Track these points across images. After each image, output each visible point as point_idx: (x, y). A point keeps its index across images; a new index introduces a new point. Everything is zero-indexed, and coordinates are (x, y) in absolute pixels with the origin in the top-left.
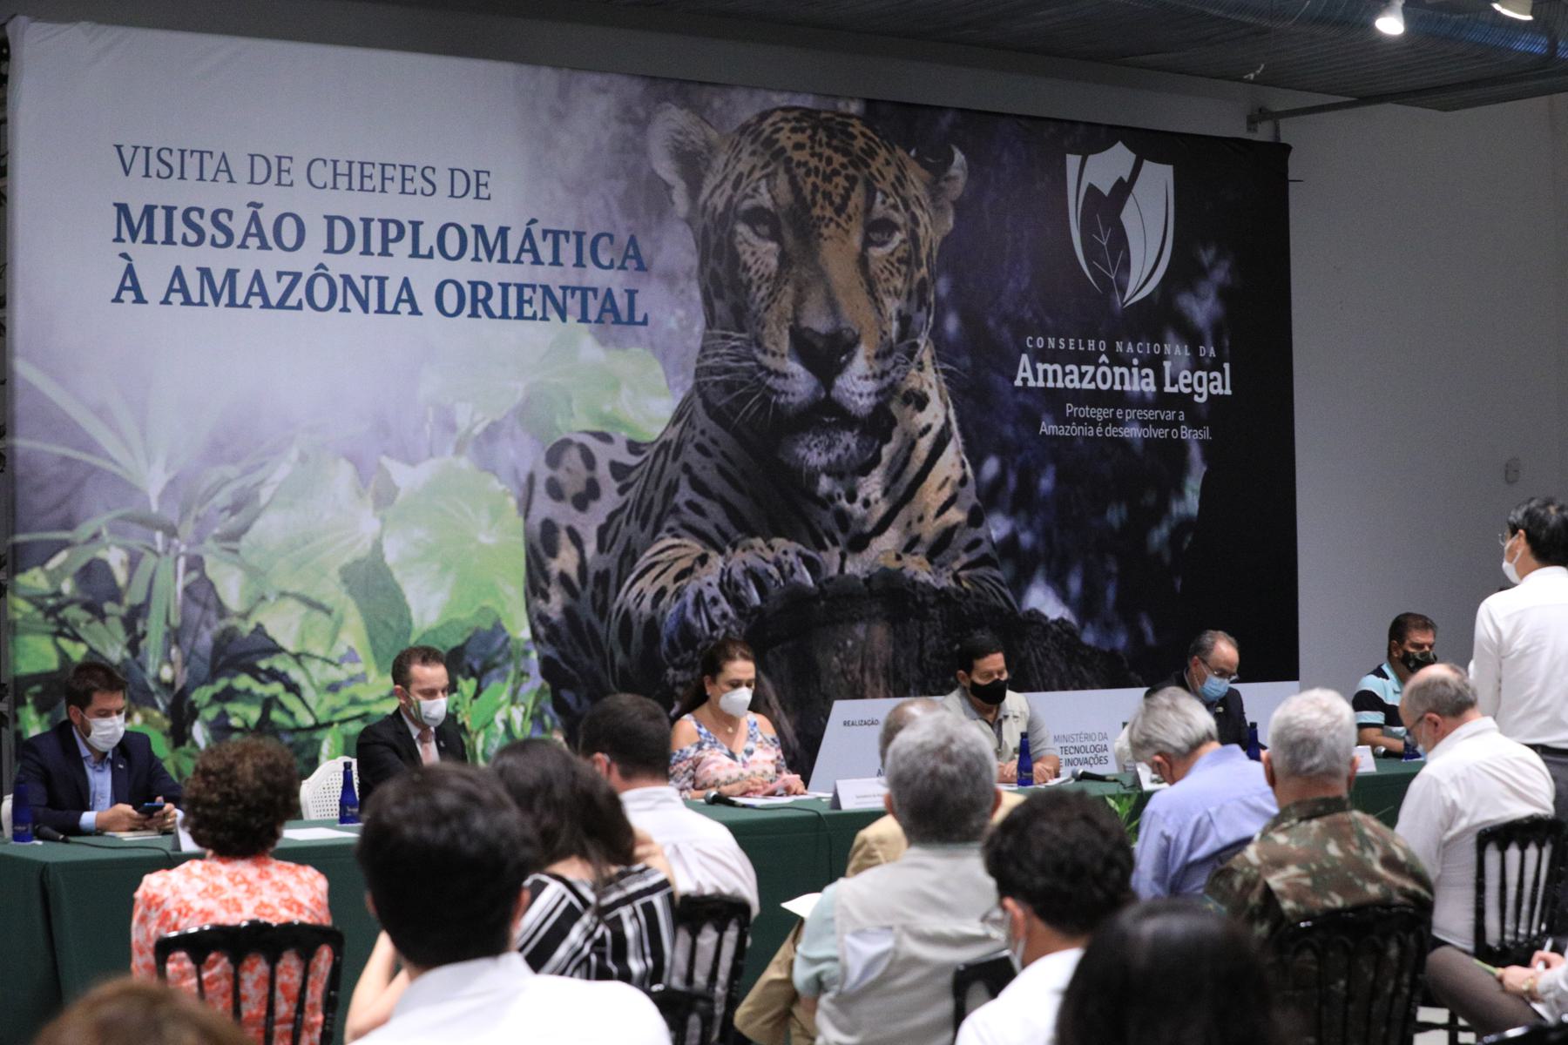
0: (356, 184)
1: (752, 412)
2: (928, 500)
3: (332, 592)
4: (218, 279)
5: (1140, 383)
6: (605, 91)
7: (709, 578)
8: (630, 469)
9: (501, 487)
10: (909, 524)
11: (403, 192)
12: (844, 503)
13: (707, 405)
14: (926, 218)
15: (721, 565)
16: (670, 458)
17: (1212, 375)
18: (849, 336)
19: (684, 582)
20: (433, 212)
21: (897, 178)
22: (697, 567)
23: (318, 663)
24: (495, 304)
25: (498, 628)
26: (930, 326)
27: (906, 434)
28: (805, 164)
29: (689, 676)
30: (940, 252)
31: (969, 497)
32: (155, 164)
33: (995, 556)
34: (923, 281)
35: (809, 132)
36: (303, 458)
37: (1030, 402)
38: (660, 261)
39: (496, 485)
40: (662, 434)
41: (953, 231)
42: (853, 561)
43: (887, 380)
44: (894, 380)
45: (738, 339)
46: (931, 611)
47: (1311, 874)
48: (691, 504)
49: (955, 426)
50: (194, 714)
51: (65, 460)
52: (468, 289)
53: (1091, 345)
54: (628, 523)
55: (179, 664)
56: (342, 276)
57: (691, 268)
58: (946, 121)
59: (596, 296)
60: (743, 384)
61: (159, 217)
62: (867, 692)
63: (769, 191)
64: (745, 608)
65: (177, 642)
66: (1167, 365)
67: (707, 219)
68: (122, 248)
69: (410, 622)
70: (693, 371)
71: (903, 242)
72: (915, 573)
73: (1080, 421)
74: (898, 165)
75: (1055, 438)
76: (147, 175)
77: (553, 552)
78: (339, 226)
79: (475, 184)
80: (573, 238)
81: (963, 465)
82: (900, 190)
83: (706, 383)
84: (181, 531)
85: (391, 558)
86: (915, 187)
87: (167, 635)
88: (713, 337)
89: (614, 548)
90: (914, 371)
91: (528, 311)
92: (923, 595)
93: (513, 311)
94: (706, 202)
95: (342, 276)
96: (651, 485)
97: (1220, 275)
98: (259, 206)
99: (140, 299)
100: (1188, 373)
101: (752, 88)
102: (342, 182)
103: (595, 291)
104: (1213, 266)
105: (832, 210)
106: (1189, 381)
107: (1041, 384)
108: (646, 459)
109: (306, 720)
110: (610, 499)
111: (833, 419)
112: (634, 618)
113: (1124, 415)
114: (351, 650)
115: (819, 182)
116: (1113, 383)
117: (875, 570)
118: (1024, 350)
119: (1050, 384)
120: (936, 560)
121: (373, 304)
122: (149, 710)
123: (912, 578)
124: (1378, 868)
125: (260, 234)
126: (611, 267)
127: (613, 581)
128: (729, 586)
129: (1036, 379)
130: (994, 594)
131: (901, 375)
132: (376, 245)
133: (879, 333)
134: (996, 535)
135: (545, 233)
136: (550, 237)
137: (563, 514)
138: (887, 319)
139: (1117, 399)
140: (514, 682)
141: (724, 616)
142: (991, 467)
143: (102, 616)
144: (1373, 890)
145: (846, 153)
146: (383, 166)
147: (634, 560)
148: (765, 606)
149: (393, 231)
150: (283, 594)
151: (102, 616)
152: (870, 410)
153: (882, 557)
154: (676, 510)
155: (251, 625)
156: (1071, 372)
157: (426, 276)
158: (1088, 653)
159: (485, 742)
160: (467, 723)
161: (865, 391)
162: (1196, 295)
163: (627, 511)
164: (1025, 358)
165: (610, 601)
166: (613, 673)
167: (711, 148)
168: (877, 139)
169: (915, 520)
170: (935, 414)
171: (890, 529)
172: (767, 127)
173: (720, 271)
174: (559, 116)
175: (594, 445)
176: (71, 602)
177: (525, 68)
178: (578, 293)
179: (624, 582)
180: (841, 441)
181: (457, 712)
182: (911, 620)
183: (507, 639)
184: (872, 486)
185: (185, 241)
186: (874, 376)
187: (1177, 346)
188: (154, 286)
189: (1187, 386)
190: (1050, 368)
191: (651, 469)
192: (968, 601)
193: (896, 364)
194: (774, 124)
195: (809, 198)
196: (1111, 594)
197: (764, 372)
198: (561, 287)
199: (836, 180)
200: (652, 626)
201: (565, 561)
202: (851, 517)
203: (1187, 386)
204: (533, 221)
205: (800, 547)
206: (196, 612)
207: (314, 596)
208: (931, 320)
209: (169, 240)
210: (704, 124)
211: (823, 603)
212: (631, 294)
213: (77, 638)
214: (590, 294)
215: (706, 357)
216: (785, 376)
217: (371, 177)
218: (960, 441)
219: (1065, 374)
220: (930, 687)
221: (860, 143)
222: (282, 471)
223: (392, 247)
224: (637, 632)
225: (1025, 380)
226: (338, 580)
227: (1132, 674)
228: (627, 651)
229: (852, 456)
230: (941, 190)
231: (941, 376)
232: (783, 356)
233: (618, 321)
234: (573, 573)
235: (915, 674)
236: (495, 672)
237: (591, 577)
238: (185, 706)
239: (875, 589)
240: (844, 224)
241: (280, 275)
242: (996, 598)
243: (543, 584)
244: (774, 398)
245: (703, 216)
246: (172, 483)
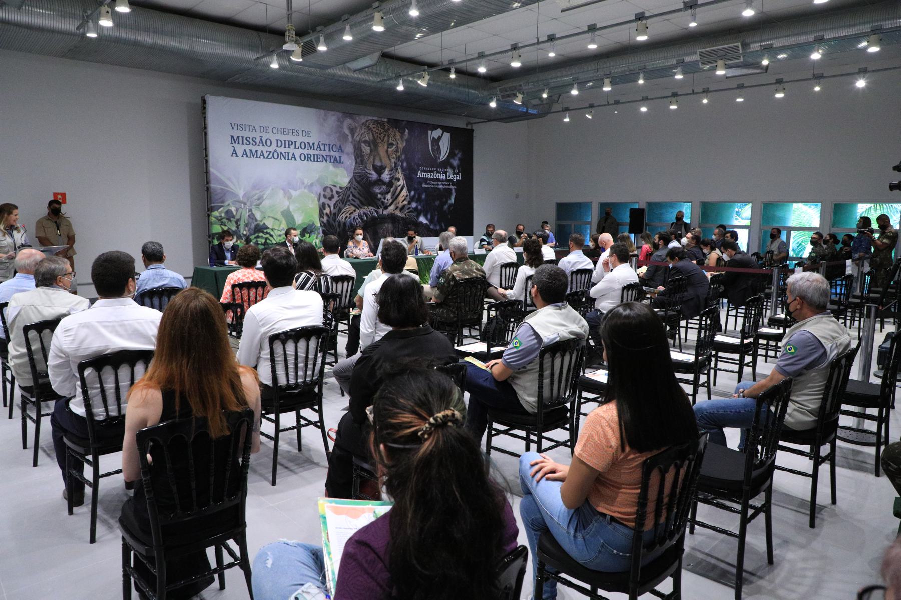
3: (279, 217)
4: (254, 153)
5: (443, 177)
6: (334, 115)
7: (356, 214)
20: (299, 140)
24: (312, 159)
25: (313, 224)
32: (239, 128)
36: (272, 190)
37: (420, 180)
39: (312, 195)
45: (362, 167)
47: (461, 272)
48: (352, 200)
51: (222, 189)
61: (240, 139)
68: (234, 145)
73: (431, 185)
75: (425, 188)
77: (325, 209)
78: (279, 142)
79: (308, 134)
85: (291, 210)
91: (319, 160)
93: (316, 160)
97: (459, 156)
99: (237, 156)
102: (280, 133)
109: (275, 243)
110: (336, 198)
121: (287, 158)
124: (475, 271)
125: (262, 143)
128: (360, 216)
132: (287, 146)
137: (327, 201)
139: (438, 180)
142: (413, 193)
143: (231, 221)
144: (474, 275)
149: (290, 143)
150: (269, 217)
151: (231, 221)
154: (350, 201)
155: (262, 223)
157: (298, 153)
167: (356, 128)
170: (402, 182)
172: (368, 124)
173: (359, 153)
174: (325, 120)
175: (332, 187)
184: (389, 197)
188: (240, 153)
196: (436, 219)
200: (345, 224)
201: (327, 211)
206: (251, 221)
207: (276, 217)
209: (243, 144)
212: (340, 157)
213: (225, 226)
221: (387, 127)
222: (268, 192)
224: (342, 225)
228: (339, 228)
233: (337, 163)
234: (329, 213)
246: (245, 194)
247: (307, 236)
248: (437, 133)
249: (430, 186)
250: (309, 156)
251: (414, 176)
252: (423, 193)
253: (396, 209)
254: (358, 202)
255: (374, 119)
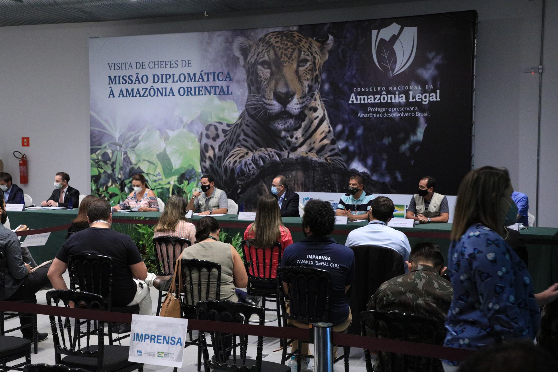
0: (160, 67)
1: (262, 115)
2: (317, 137)
3: (155, 160)
4: (130, 91)
6: (221, 36)
8: (228, 131)
9: (195, 136)
10: (310, 144)
11: (170, 67)
12: (289, 139)
13: (249, 115)
14: (319, 57)
15: (252, 155)
16: (238, 128)
17: (431, 95)
18: (292, 93)
19: (242, 159)
20: (177, 71)
21: (309, 47)
22: (245, 155)
23: (152, 176)
24: (193, 92)
25: (193, 169)
26: (319, 88)
27: (310, 119)
28: (279, 47)
29: (243, 183)
30: (323, 66)
31: (331, 136)
32: (116, 67)
33: (340, 153)
34: (317, 75)
35: (280, 38)
36: (148, 130)
37: (354, 108)
38: (236, 78)
39: (193, 135)
40: (236, 121)
41: (327, 60)
42: (292, 154)
43: (304, 104)
44: (306, 104)
45: (258, 96)
46: (317, 168)
48: (244, 139)
49: (327, 116)
50: (125, 185)
51: (99, 131)
52: (186, 89)
53: (379, 89)
54: (226, 144)
55: (122, 175)
56: (157, 88)
57: (244, 79)
58: (326, 28)
59: (218, 88)
60: (259, 108)
61: (117, 78)
62: (296, 190)
63: (268, 56)
64: (259, 166)
65: (122, 170)
66: (411, 93)
67: (249, 65)
68: (110, 86)
69: (172, 167)
70: (245, 105)
71: (311, 65)
72: (312, 158)
73: (373, 113)
74: (309, 43)
76: (115, 69)
77: (207, 151)
79: (188, 64)
80: (212, 74)
81: (329, 127)
82: (310, 50)
83: (248, 108)
84: (123, 146)
85: (168, 152)
86: (315, 48)
87: (120, 168)
88: (251, 96)
89: (223, 150)
90: (313, 101)
91: (201, 93)
92: (314, 164)
93: (197, 93)
94: (249, 61)
95: (157, 88)
96: (233, 133)
98: (138, 74)
99: (114, 96)
100: (420, 95)
101: (263, 28)
102: (156, 66)
103: (218, 87)
104: (433, 58)
105: (287, 58)
106: (420, 97)
107: (359, 102)
108: (232, 128)
110: (222, 138)
111: (286, 116)
112: (228, 168)
113: (392, 110)
114: (159, 173)
115: (283, 51)
116: (388, 100)
117: (299, 157)
118: (353, 92)
119: (362, 102)
120: (319, 154)
121: (164, 94)
122: (116, 184)
123: (311, 159)
125: (139, 80)
126: (222, 80)
127: (223, 158)
128: (254, 160)
129: (357, 100)
130: (339, 164)
131: (309, 102)
132: (164, 81)
133: (302, 91)
134: (340, 147)
135: (205, 73)
136: (206, 74)
137: (210, 142)
138: (304, 87)
140: (197, 182)
141: (253, 168)
142: (339, 127)
143: (107, 164)
145: (292, 42)
146: (166, 62)
147: (228, 153)
148: (265, 166)
149: (168, 77)
150: (144, 160)
151: (107, 164)
152: (298, 113)
153: (301, 153)
154: (240, 141)
155: (137, 167)
156: (371, 98)
157: (176, 87)
158: (374, 183)
159: (190, 196)
160: (186, 191)
161: (297, 108)
162: (425, 69)
163: (226, 141)
164: (353, 95)
165: (222, 163)
166: (222, 181)
167: (250, 46)
168: (302, 36)
169: (312, 143)
170: (320, 113)
171: (304, 145)
172: (267, 38)
173: (253, 79)
174: (208, 44)
175: (218, 125)
176: (101, 161)
177: (200, 33)
178: (214, 88)
179: (226, 158)
180: (288, 122)
181: (183, 188)
182: (310, 171)
183: (196, 172)
184: (299, 134)
185: (123, 83)
186: (300, 103)
187: (416, 86)
188: (117, 93)
189: (419, 99)
190: (362, 97)
191: (233, 131)
192: (330, 166)
193: (307, 100)
194: (269, 37)
195: (280, 56)
196: (384, 165)
197: (265, 104)
198: (209, 87)
199: (289, 50)
200: (233, 170)
201: (210, 153)
202: (291, 142)
203: (419, 99)
204: (202, 71)
205: (275, 150)
206: (126, 163)
207: (151, 161)
208: (319, 86)
209: (119, 83)
210: (248, 40)
211: (282, 165)
212: (228, 87)
213: (102, 168)
214: (217, 88)
215: (248, 101)
216: (272, 105)
217: (163, 64)
218: (328, 120)
219: (368, 99)
220: (316, 189)
222: (144, 133)
223: (168, 81)
224: (229, 171)
225: (353, 101)
226: (156, 157)
227: (392, 190)
228: (226, 176)
229: (292, 126)
230: (324, 48)
231: (322, 102)
232: (271, 100)
233: (224, 94)
234: (212, 156)
235: (311, 186)
236: (192, 179)
237: (217, 157)
238: (123, 184)
239: (299, 161)
240: (291, 62)
241: (143, 89)
242: (340, 165)
243: (204, 159)
244: (268, 111)
245: (248, 65)
246: (121, 136)
247: (186, 182)
248: (386, 33)
249: (372, 115)
250: (189, 89)
251: (343, 102)
252: (359, 127)
253: (310, 151)
254: (251, 142)
255: (277, 29)
